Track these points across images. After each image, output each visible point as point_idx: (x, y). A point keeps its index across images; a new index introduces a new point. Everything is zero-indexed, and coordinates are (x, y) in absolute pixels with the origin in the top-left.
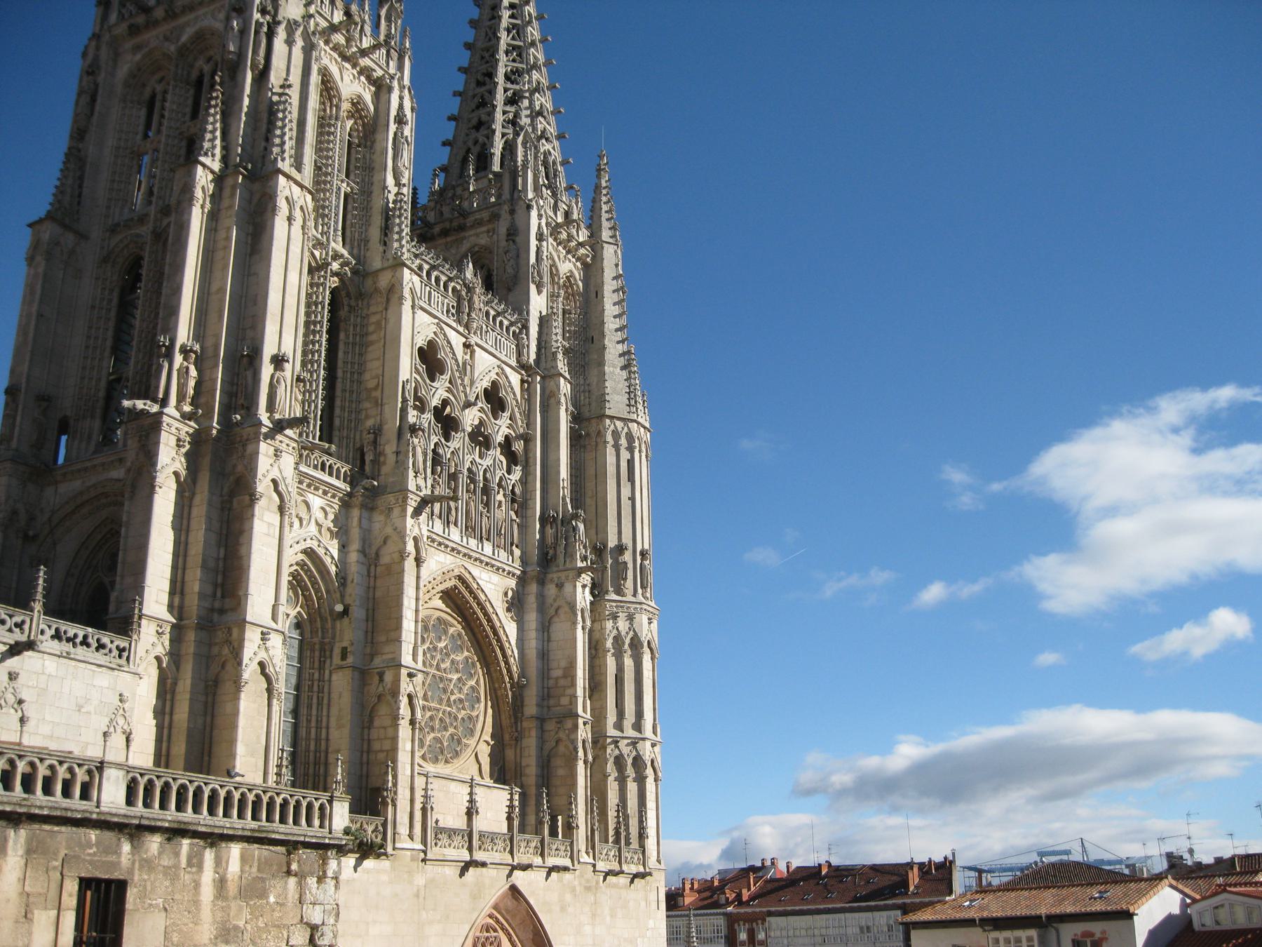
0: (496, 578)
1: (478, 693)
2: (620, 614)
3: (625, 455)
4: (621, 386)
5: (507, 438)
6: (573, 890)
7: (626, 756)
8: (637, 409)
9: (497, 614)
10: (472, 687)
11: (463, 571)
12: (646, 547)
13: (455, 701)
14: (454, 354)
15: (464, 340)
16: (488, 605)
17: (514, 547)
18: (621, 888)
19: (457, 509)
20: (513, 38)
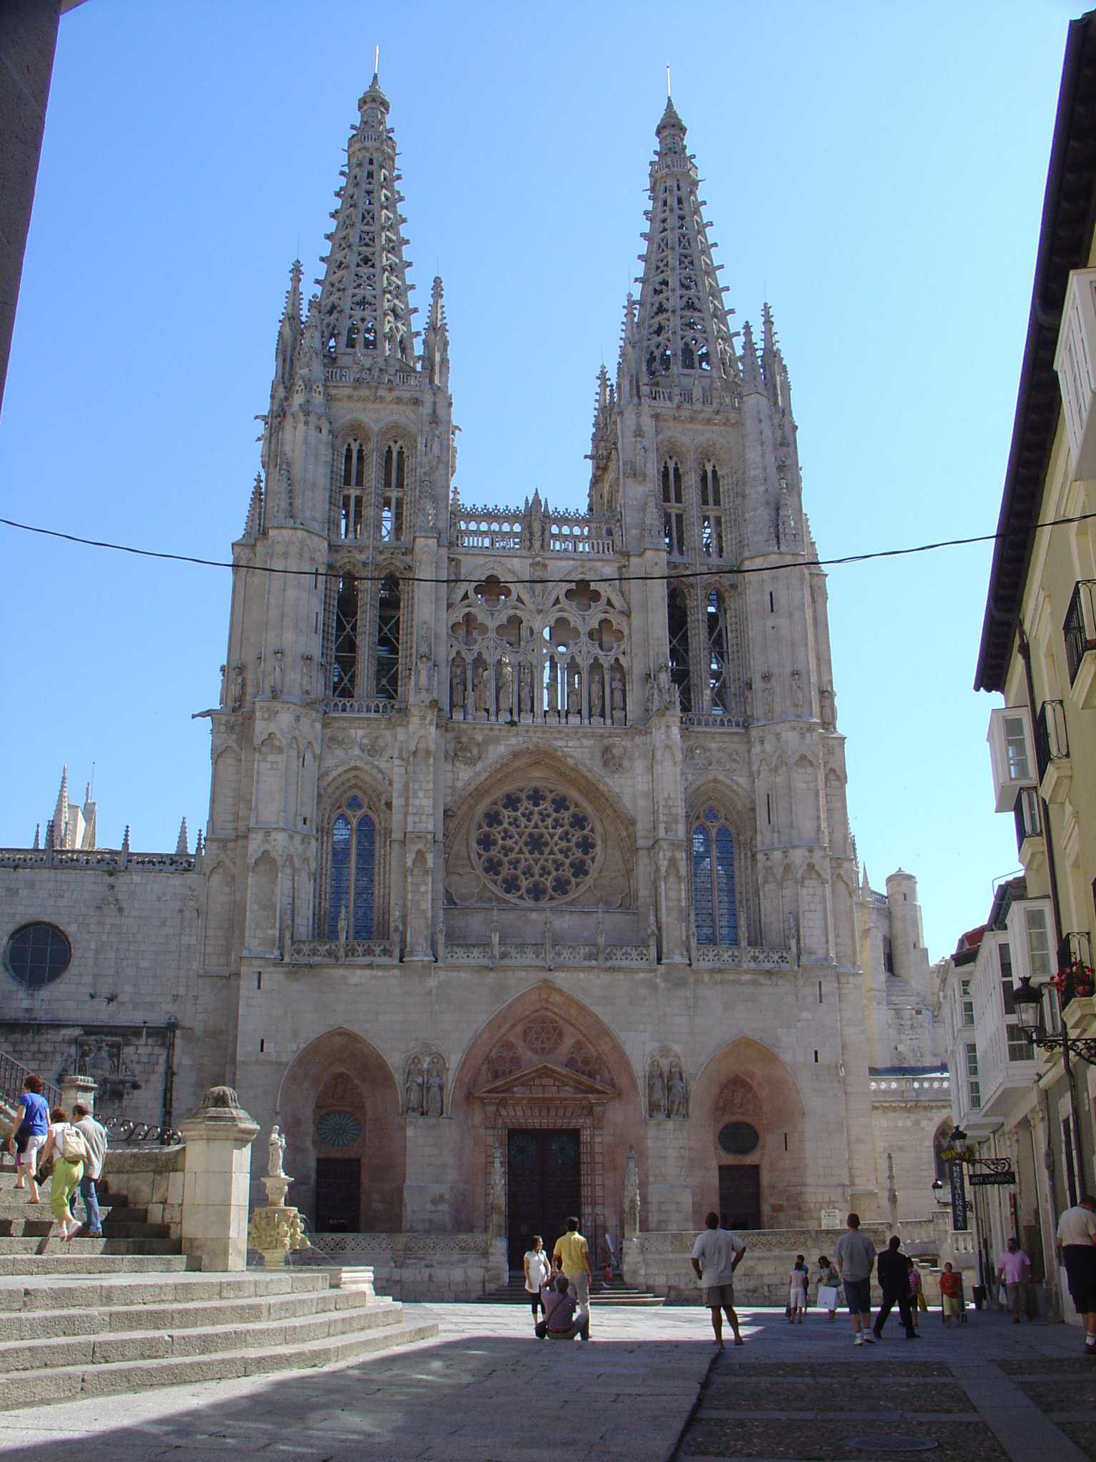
0: (588, 742)
5: (604, 622)
6: (653, 987)
8: (778, 543)
15: (531, 561)
18: (743, 984)
20: (663, 251)
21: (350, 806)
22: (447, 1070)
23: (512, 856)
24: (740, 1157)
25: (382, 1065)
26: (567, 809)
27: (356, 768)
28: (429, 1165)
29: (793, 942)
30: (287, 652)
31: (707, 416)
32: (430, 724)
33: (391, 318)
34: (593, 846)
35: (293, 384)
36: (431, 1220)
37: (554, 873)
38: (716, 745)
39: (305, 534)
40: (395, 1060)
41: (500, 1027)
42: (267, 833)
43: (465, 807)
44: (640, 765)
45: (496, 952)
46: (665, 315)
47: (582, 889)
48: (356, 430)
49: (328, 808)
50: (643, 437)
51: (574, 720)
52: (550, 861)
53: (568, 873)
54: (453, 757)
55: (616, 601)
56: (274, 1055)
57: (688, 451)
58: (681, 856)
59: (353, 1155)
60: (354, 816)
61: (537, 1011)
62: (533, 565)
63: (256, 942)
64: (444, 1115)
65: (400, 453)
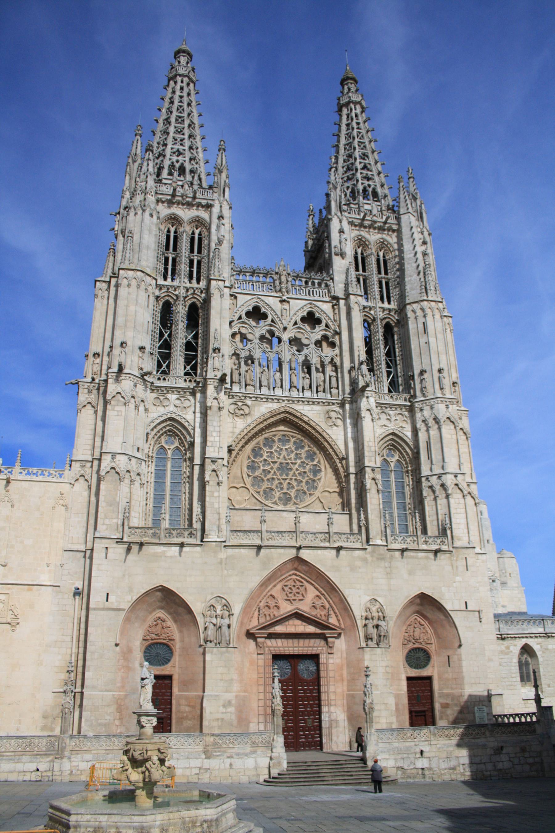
0: (317, 408)
1: (319, 467)
2: (425, 408)
3: (421, 320)
4: (415, 285)
5: (325, 338)
6: (365, 560)
7: (435, 486)
8: (427, 293)
10: (315, 465)
11: (287, 408)
12: (444, 365)
13: (300, 474)
14: (271, 307)
15: (280, 299)
16: (312, 422)
17: (332, 390)
19: (282, 380)
20: (348, 140)
22: (233, 615)
23: (270, 476)
24: (419, 671)
25: (190, 611)
28: (221, 680)
29: (449, 532)
30: (129, 343)
31: (379, 224)
33: (194, 164)
34: (320, 471)
35: (135, 191)
36: (222, 719)
38: (393, 412)
39: (142, 274)
40: (197, 607)
41: (267, 587)
45: (265, 535)
46: (351, 173)
47: (314, 498)
48: (174, 220)
49: (153, 444)
50: (343, 232)
51: (308, 394)
52: (293, 480)
54: (234, 414)
55: (330, 324)
56: (116, 604)
57: (370, 244)
58: (379, 476)
59: (167, 673)
60: (169, 449)
61: (290, 575)
63: (104, 527)
64: (231, 645)
65: (200, 234)
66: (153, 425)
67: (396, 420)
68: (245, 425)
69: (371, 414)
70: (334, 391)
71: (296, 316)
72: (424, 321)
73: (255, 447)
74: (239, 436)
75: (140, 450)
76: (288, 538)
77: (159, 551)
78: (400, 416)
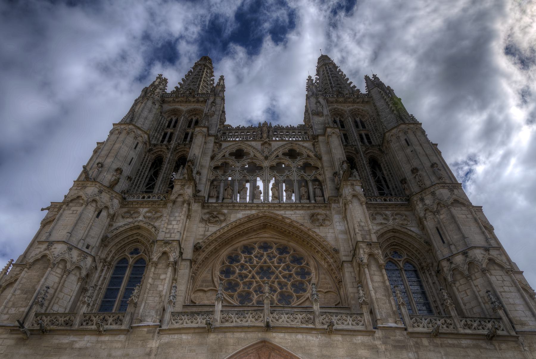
9: (302, 225)
15: (262, 142)
16: (295, 224)
21: (132, 253)
26: (288, 253)
27: (139, 228)
32: (188, 188)
34: (309, 273)
37: (279, 290)
38: (390, 212)
42: (51, 243)
43: (212, 247)
44: (336, 218)
48: (176, 112)
49: (113, 252)
52: (276, 283)
53: (289, 289)
55: (312, 154)
62: (262, 145)
66: (115, 232)
67: (394, 219)
68: (218, 228)
69: (359, 199)
70: (318, 199)
71: (277, 152)
72: (406, 137)
73: (232, 253)
74: (210, 238)
75: (90, 248)
76: (253, 320)
77: (67, 341)
78: (399, 216)
